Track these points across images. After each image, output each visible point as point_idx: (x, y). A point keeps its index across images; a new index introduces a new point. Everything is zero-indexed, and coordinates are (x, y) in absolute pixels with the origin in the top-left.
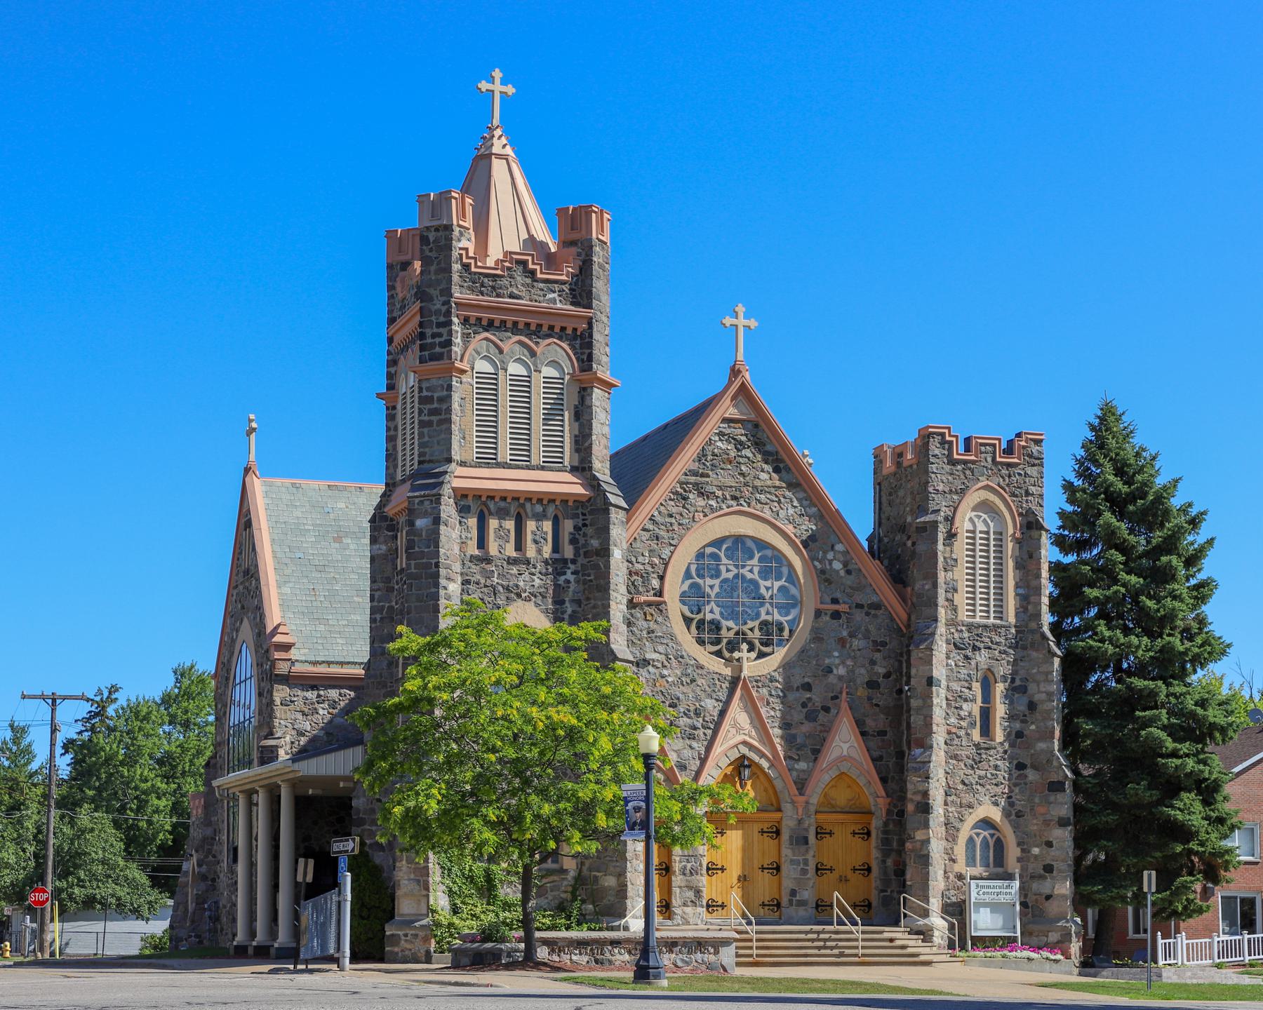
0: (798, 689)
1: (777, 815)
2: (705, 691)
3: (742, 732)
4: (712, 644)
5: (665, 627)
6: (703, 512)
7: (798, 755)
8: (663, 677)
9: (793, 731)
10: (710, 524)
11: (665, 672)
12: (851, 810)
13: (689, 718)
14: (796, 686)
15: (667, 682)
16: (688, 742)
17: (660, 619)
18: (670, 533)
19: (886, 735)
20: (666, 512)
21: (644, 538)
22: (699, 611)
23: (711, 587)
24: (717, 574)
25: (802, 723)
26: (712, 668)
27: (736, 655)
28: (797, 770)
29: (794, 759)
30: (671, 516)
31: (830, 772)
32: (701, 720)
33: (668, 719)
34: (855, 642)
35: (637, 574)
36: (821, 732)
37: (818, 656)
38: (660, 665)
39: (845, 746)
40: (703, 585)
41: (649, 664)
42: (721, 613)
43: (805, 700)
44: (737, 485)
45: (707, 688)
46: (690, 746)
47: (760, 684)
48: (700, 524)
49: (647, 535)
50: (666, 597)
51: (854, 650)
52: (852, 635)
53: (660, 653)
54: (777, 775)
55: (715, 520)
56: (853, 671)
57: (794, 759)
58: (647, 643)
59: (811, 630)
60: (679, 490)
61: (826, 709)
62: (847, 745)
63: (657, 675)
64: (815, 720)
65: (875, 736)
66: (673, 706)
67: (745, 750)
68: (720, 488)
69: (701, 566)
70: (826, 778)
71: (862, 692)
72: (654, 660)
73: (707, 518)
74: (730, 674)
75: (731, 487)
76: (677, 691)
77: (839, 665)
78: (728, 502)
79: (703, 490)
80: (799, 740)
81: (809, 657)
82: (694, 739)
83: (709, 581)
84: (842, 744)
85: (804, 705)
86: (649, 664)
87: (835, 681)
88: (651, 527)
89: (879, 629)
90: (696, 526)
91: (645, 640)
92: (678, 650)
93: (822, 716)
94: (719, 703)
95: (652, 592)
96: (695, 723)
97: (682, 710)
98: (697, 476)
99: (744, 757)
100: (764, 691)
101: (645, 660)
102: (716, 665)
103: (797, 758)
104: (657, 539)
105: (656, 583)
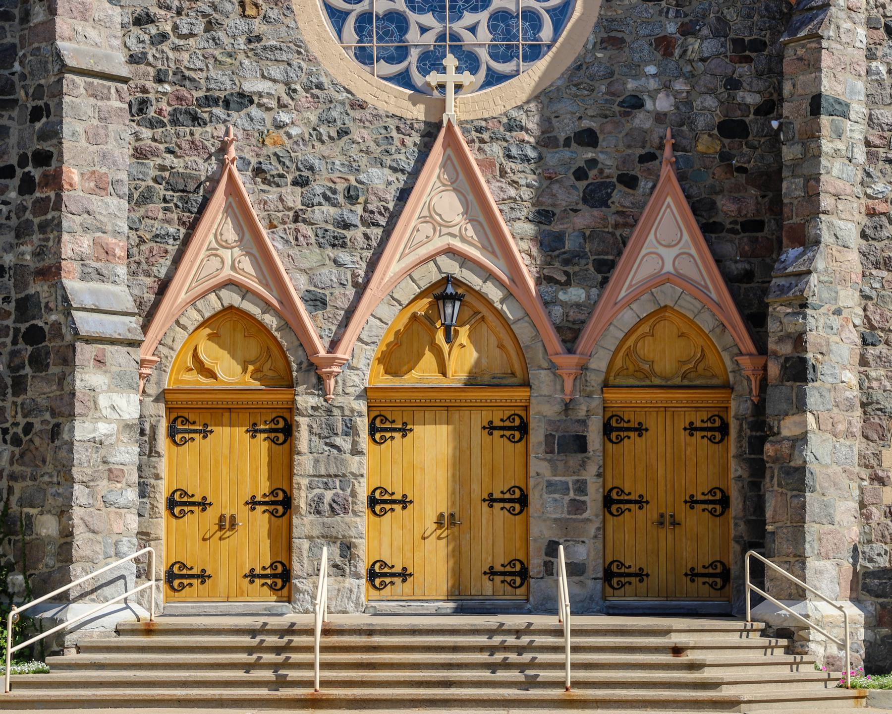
0: (567, 143)
1: (521, 394)
2: (368, 152)
3: (445, 230)
5: (283, 29)
7: (566, 273)
8: (279, 126)
9: (556, 227)
11: (284, 117)
12: (686, 382)
13: (334, 205)
14: (562, 136)
15: (289, 136)
16: (330, 252)
17: (273, 14)
19: (762, 230)
25: (575, 211)
26: (383, 107)
27: (434, 78)
28: (563, 304)
29: (557, 282)
31: (634, 306)
32: (359, 209)
33: (290, 209)
34: (694, 44)
36: (616, 226)
37: (612, 74)
38: (273, 104)
39: (669, 255)
41: (251, 102)
43: (582, 164)
45: (373, 146)
46: (335, 261)
47: (486, 136)
51: (690, 61)
52: (687, 30)
54: (520, 314)
56: (689, 103)
57: (557, 282)
58: (246, 62)
59: (598, 24)
61: (631, 182)
62: (675, 251)
63: (268, 123)
64: (604, 203)
65: (735, 232)
67: (451, 267)
70: (628, 318)
71: (707, 145)
72: (260, 95)
74: (422, 117)
76: (309, 154)
77: (658, 91)
80: (568, 245)
81: (592, 78)
82: (344, 246)
84: (662, 251)
85: (580, 174)
86: (251, 102)
87: (648, 124)
89: (749, 16)
91: (241, 57)
92: (310, 74)
93: (620, 197)
97: (319, 190)
99: (448, 279)
100: (496, 150)
101: (241, 95)
102: (392, 100)
103: (563, 279)
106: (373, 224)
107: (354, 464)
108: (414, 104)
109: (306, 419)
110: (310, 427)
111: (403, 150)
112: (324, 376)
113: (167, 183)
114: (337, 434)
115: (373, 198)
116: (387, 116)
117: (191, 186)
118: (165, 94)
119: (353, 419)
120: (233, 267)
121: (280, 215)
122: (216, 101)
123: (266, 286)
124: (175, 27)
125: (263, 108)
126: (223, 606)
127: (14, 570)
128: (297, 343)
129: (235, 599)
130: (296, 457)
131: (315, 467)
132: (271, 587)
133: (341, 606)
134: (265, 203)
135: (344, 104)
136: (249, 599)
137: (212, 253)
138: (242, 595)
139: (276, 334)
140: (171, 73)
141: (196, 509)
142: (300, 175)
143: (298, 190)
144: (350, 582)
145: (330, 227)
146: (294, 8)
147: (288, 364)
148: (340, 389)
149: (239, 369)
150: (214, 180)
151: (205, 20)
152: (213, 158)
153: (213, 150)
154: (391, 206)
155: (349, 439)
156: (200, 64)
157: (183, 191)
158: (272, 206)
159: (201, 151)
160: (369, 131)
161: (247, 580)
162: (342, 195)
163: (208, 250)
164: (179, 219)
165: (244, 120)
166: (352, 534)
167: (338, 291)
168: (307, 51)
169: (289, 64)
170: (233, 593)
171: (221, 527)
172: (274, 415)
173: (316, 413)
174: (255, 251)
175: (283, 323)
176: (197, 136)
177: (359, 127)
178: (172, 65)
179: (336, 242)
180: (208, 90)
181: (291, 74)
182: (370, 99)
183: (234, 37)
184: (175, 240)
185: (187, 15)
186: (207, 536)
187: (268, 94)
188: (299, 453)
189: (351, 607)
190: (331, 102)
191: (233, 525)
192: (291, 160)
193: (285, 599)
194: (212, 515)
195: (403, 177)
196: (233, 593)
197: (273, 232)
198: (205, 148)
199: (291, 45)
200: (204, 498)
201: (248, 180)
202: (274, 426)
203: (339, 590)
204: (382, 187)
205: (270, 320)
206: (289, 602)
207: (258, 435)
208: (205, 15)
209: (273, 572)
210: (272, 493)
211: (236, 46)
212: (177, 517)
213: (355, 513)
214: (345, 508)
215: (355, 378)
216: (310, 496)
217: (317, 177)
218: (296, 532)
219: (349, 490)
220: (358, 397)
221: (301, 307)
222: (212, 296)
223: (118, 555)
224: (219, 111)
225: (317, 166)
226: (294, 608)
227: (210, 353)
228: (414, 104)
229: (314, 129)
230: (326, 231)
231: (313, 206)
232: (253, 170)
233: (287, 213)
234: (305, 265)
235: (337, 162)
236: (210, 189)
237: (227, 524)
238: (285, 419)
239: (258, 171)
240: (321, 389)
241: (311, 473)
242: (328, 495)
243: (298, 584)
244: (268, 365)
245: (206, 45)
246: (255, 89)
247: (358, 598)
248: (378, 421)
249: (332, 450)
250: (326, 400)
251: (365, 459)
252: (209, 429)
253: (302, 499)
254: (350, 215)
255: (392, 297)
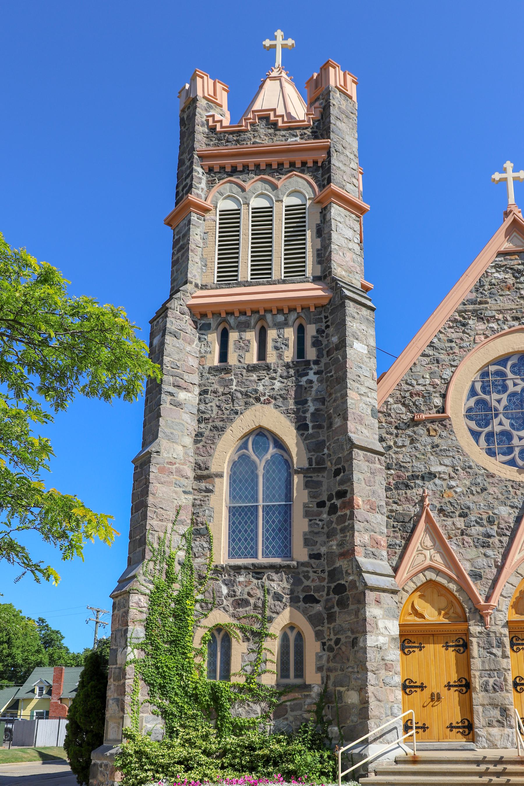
2: (497, 499)
4: (504, 454)
5: (450, 441)
6: (484, 334)
8: (450, 488)
10: (491, 344)
11: (453, 483)
13: (482, 526)
15: (456, 492)
17: (444, 434)
18: (451, 356)
20: (446, 338)
21: (424, 363)
22: (487, 425)
23: (499, 401)
24: (505, 388)
26: (503, 476)
30: (451, 341)
32: (495, 527)
33: (459, 529)
35: (418, 394)
38: (447, 477)
40: (489, 400)
41: (435, 477)
42: (512, 425)
44: (517, 307)
45: (500, 496)
48: (479, 345)
49: (427, 360)
50: (449, 412)
53: (447, 466)
55: (498, 340)
58: (432, 457)
60: (458, 317)
63: (445, 486)
66: (463, 515)
68: (500, 311)
69: (486, 384)
72: (440, 473)
73: (488, 339)
75: (511, 309)
76: (467, 501)
78: (509, 323)
79: (482, 316)
82: (489, 546)
83: (495, 396)
86: (435, 477)
88: (431, 353)
90: (476, 347)
91: (429, 455)
94: (515, 510)
95: (435, 410)
96: (489, 530)
97: (473, 519)
98: (475, 304)
101: (430, 473)
102: (508, 473)
104: (438, 362)
105: (438, 402)
106: (503, 535)
107: (504, 663)
108: (520, 474)
109: (476, 639)
110: (478, 643)
111: (516, 497)
112: (484, 615)
113: (394, 518)
114: (493, 647)
115: (502, 521)
116: (506, 481)
117: (407, 520)
118: (391, 475)
119: (502, 638)
120: (431, 559)
121: (453, 532)
122: (417, 477)
123: (449, 568)
124: (395, 443)
125: (442, 479)
126: (437, 745)
127: (331, 724)
128: (468, 598)
129: (443, 741)
130: (472, 660)
131: (482, 665)
132: (462, 733)
133: (503, 744)
134: (446, 526)
135: (483, 475)
136: (450, 740)
137: (419, 552)
138: (446, 738)
139: (456, 593)
140: (394, 465)
141: (418, 690)
142: (463, 512)
143: (462, 519)
144: (507, 730)
145: (480, 537)
146: (454, 430)
147: (463, 609)
148: (493, 622)
149: (436, 613)
150: (419, 516)
151: (410, 439)
152: (417, 505)
153: (417, 501)
154: (512, 525)
155: (500, 650)
156: (408, 460)
157: (403, 522)
158: (449, 528)
159: (411, 502)
160: (497, 488)
161: (449, 729)
162: (485, 521)
163: (417, 551)
164: (401, 536)
165: (432, 486)
166: (507, 703)
167: (487, 570)
168: (462, 451)
169: (454, 458)
170: (441, 737)
171: (432, 700)
172: (457, 637)
173: (481, 636)
174: (442, 551)
175: (459, 588)
176: (408, 495)
177: (492, 486)
178: (394, 461)
179: (485, 545)
180: (413, 472)
181: (455, 462)
182: (496, 472)
183: (425, 446)
184: (400, 546)
185: (401, 437)
186: (425, 705)
187: (444, 472)
188: (473, 658)
189: (509, 745)
190: (476, 475)
191: (439, 698)
192: (458, 504)
193: (471, 740)
194: (427, 693)
195: (517, 511)
196: (441, 737)
197: (450, 541)
198: (413, 500)
199: (454, 448)
200: (422, 684)
201: (436, 515)
202: (457, 644)
203: (502, 735)
204: (506, 516)
205: (452, 587)
206: (474, 742)
207: (449, 648)
208: (410, 436)
209: (463, 725)
210: (459, 680)
211: (426, 450)
212: (408, 694)
213: (507, 691)
214: (501, 688)
215: (501, 616)
216: (481, 682)
217: (472, 512)
218: (475, 702)
219: (502, 678)
220: (503, 626)
221: (469, 579)
222: (421, 575)
223: (394, 715)
224: (418, 482)
225: (471, 507)
226: (477, 745)
227: (421, 606)
228: (520, 474)
229: (469, 488)
230: (479, 539)
231: (471, 527)
232: (438, 510)
233: (457, 531)
234: (469, 557)
235: (482, 504)
236: (417, 520)
237: (435, 698)
238: (463, 640)
239: (441, 511)
240: (483, 622)
241: (481, 668)
242: (491, 681)
243: (478, 732)
244: (452, 611)
245: (411, 450)
246: (437, 470)
247: (513, 740)
248: (514, 639)
249: (491, 656)
250: (486, 628)
251: (509, 660)
252: (422, 645)
253: (477, 683)
254: (491, 531)
255: (517, 572)
